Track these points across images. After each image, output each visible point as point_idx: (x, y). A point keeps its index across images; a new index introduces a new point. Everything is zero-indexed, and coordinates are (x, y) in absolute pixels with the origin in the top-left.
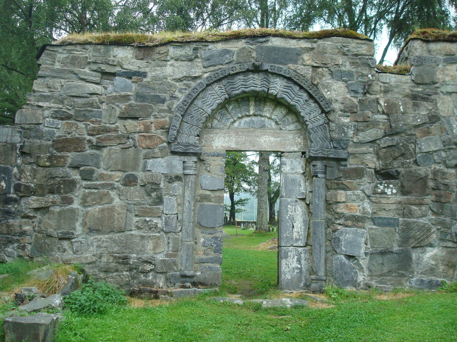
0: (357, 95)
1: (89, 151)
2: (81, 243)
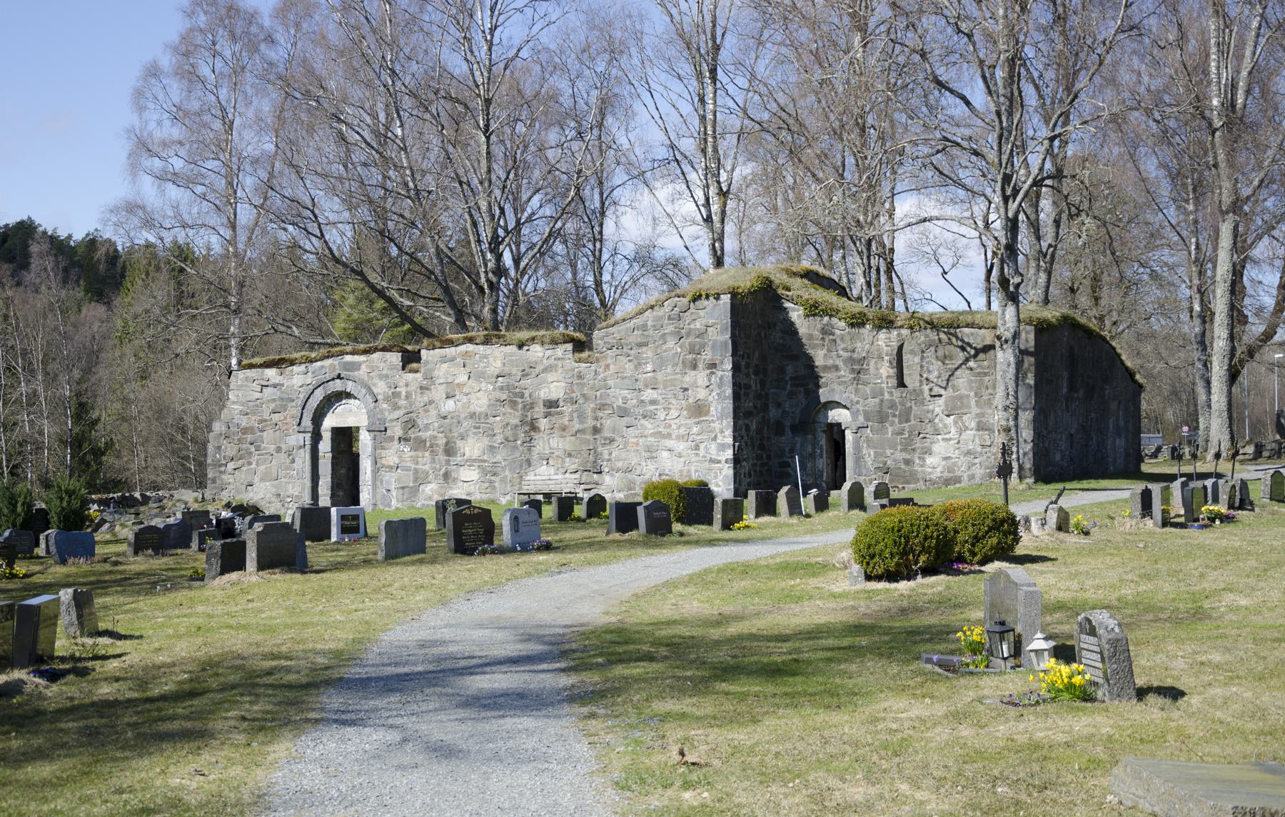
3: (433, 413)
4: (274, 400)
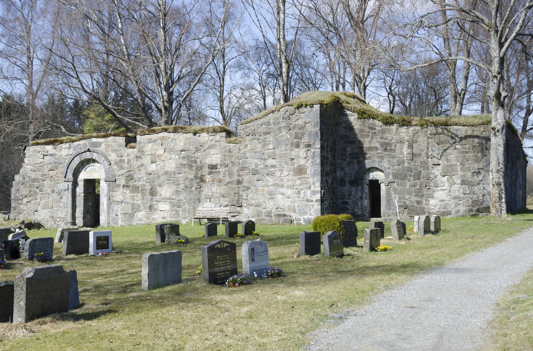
3: (143, 171)
4: (51, 163)
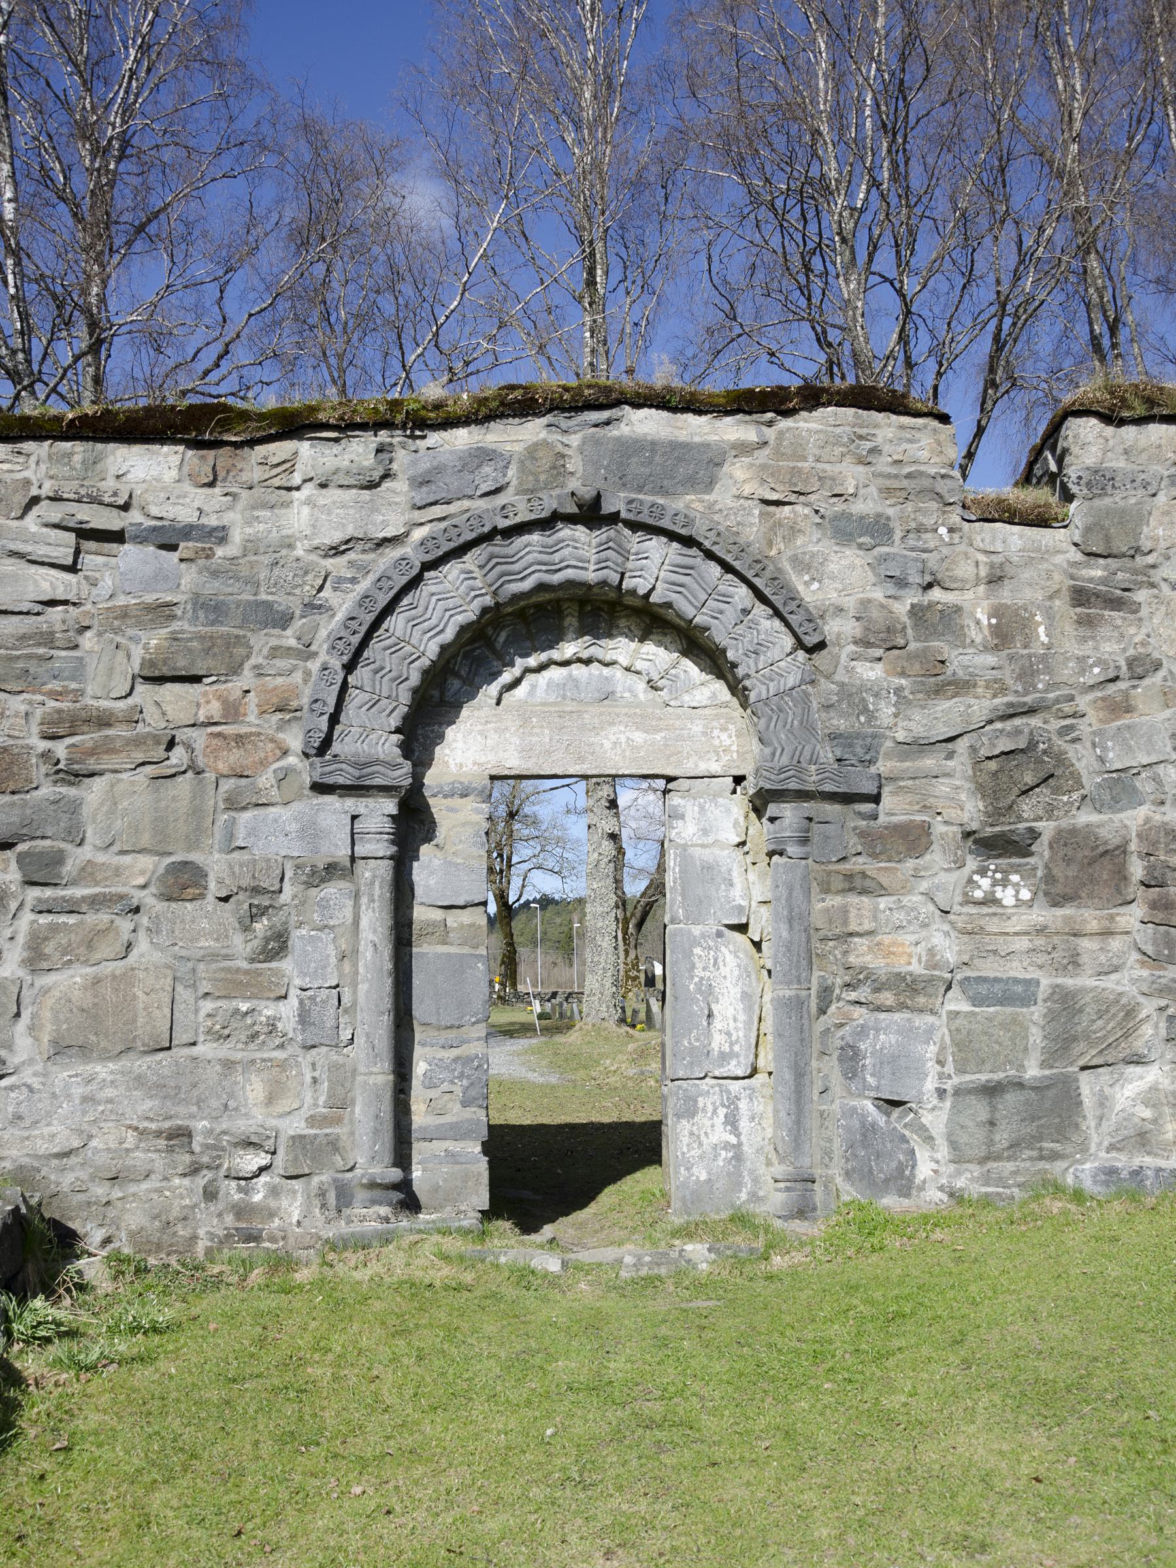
0: (902, 593)
1: (47, 790)
2: (31, 1089)
4: (162, 612)
